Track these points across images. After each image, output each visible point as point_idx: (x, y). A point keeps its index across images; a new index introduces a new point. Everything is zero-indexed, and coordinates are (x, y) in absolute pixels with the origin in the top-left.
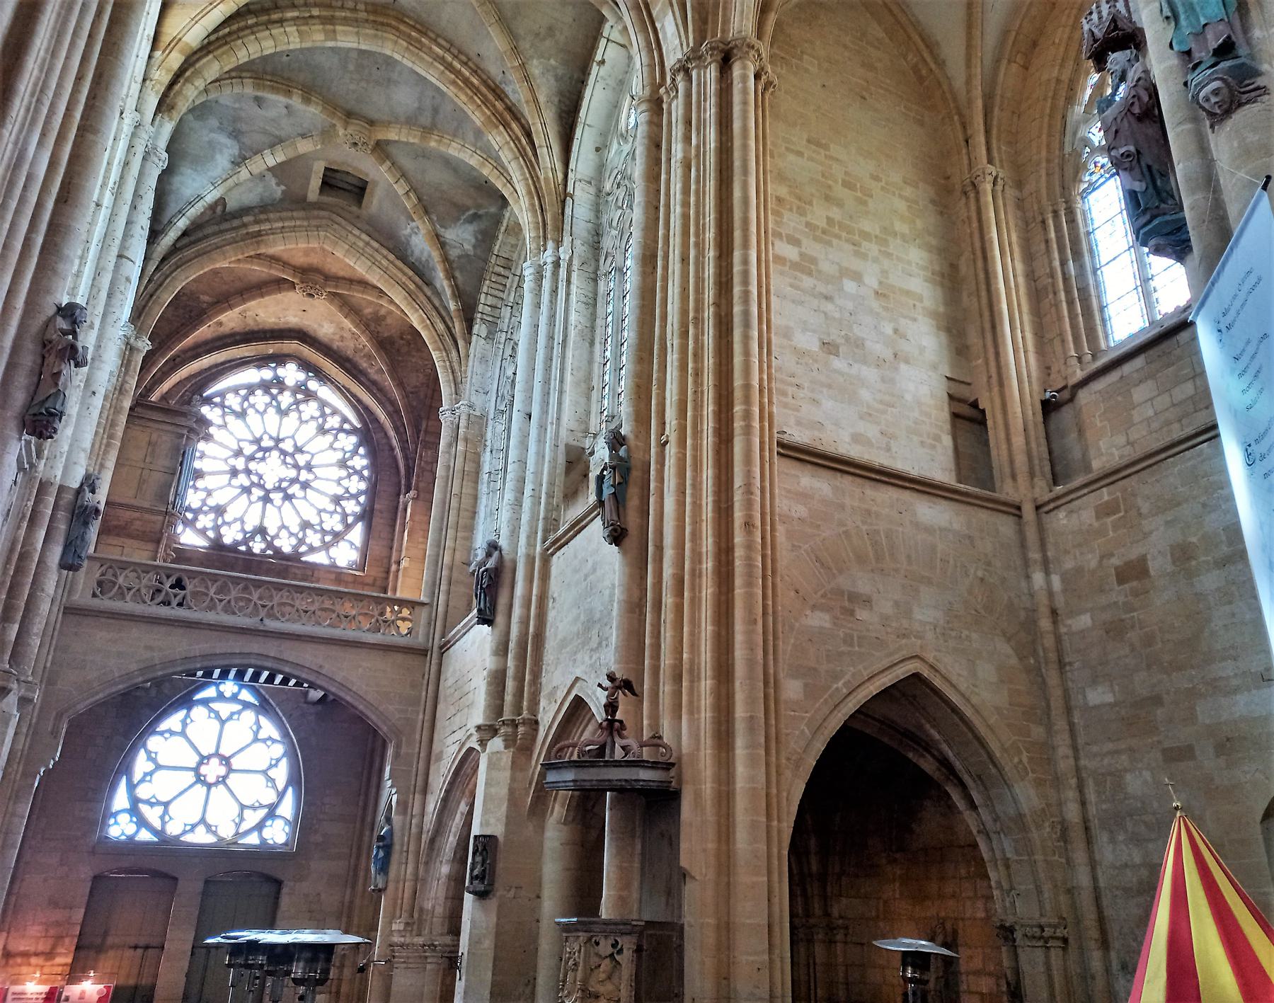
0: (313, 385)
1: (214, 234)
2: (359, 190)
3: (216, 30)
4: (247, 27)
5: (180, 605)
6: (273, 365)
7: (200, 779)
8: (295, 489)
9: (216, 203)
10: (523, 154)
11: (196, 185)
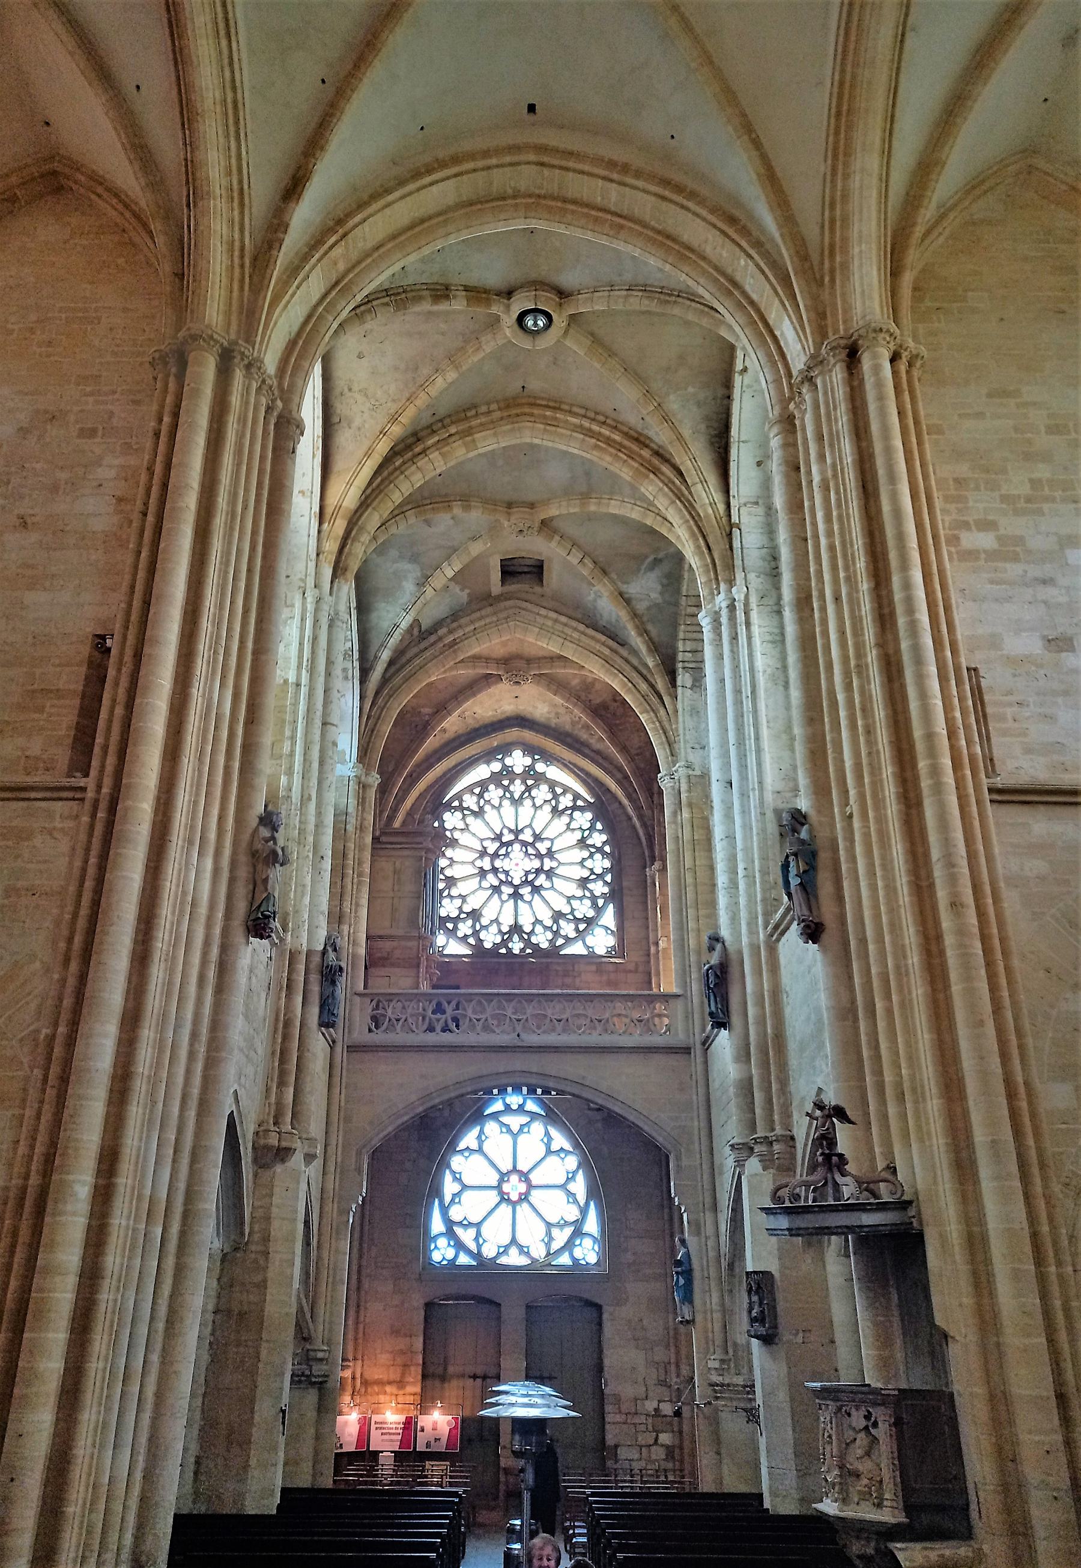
0: (540, 767)
1: (416, 655)
2: (537, 570)
3: (366, 488)
4: (396, 469)
5: (444, 1030)
6: (500, 757)
7: (504, 1198)
8: (541, 880)
9: (411, 627)
10: (679, 496)
11: (390, 615)
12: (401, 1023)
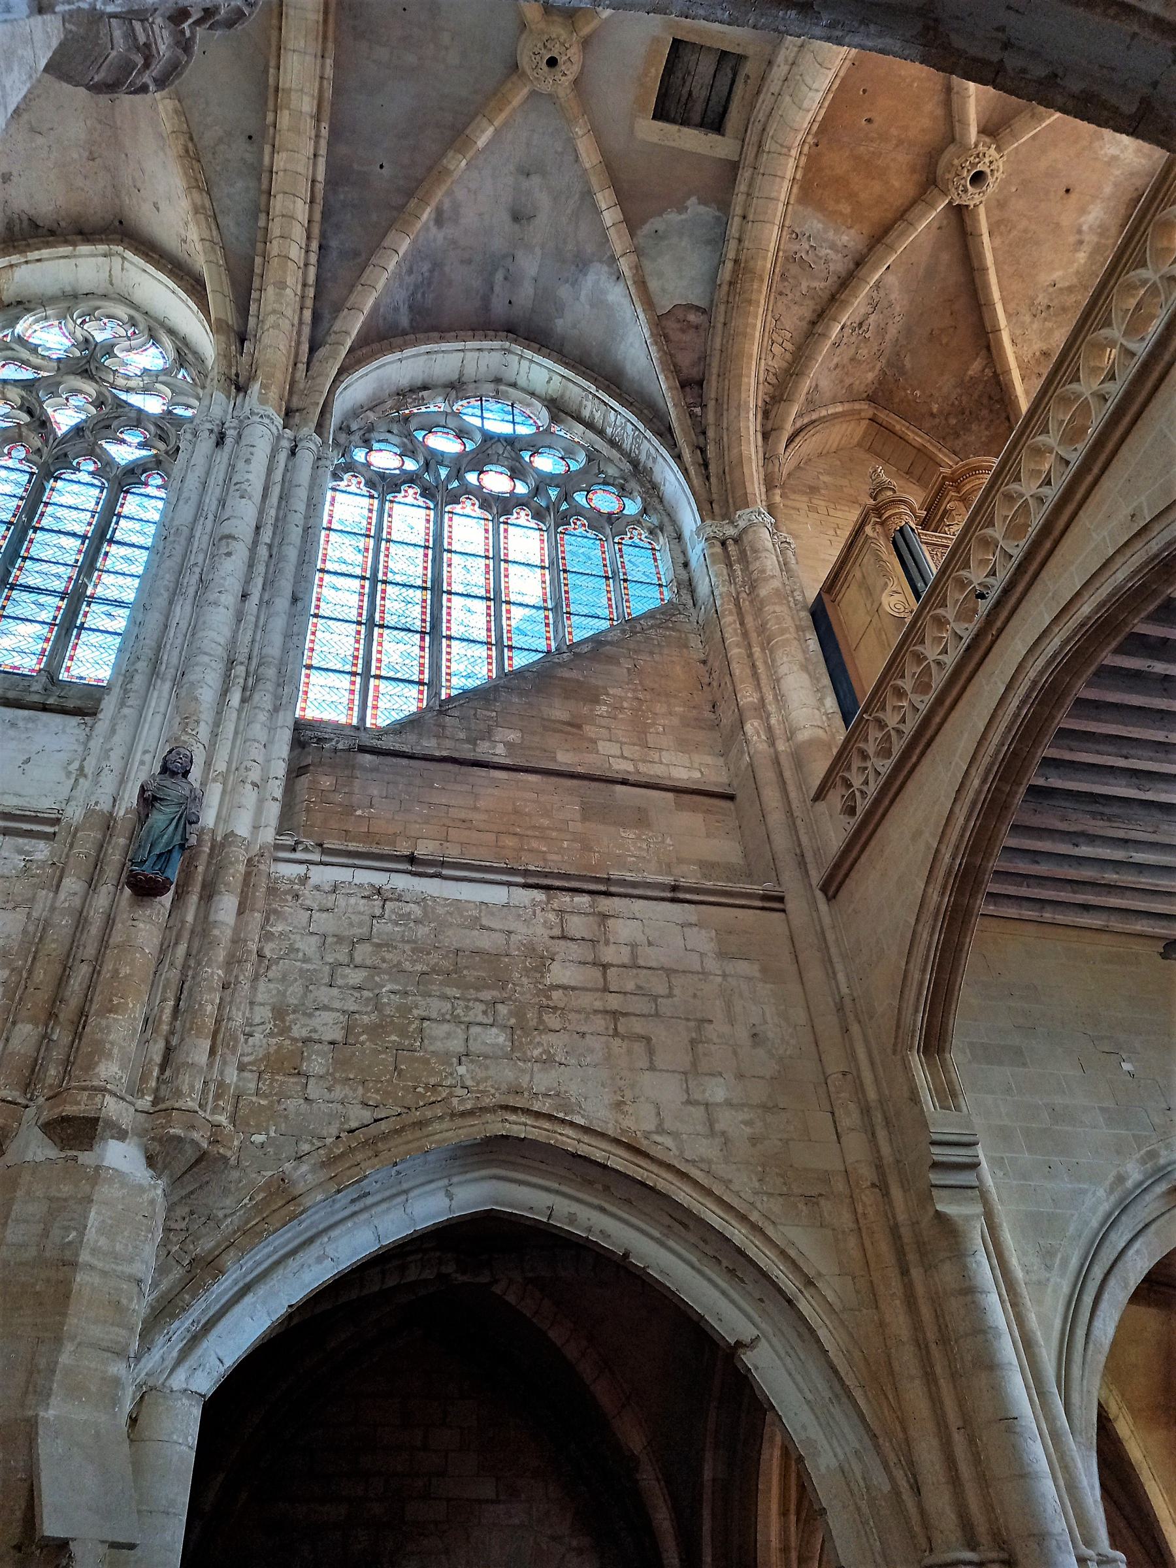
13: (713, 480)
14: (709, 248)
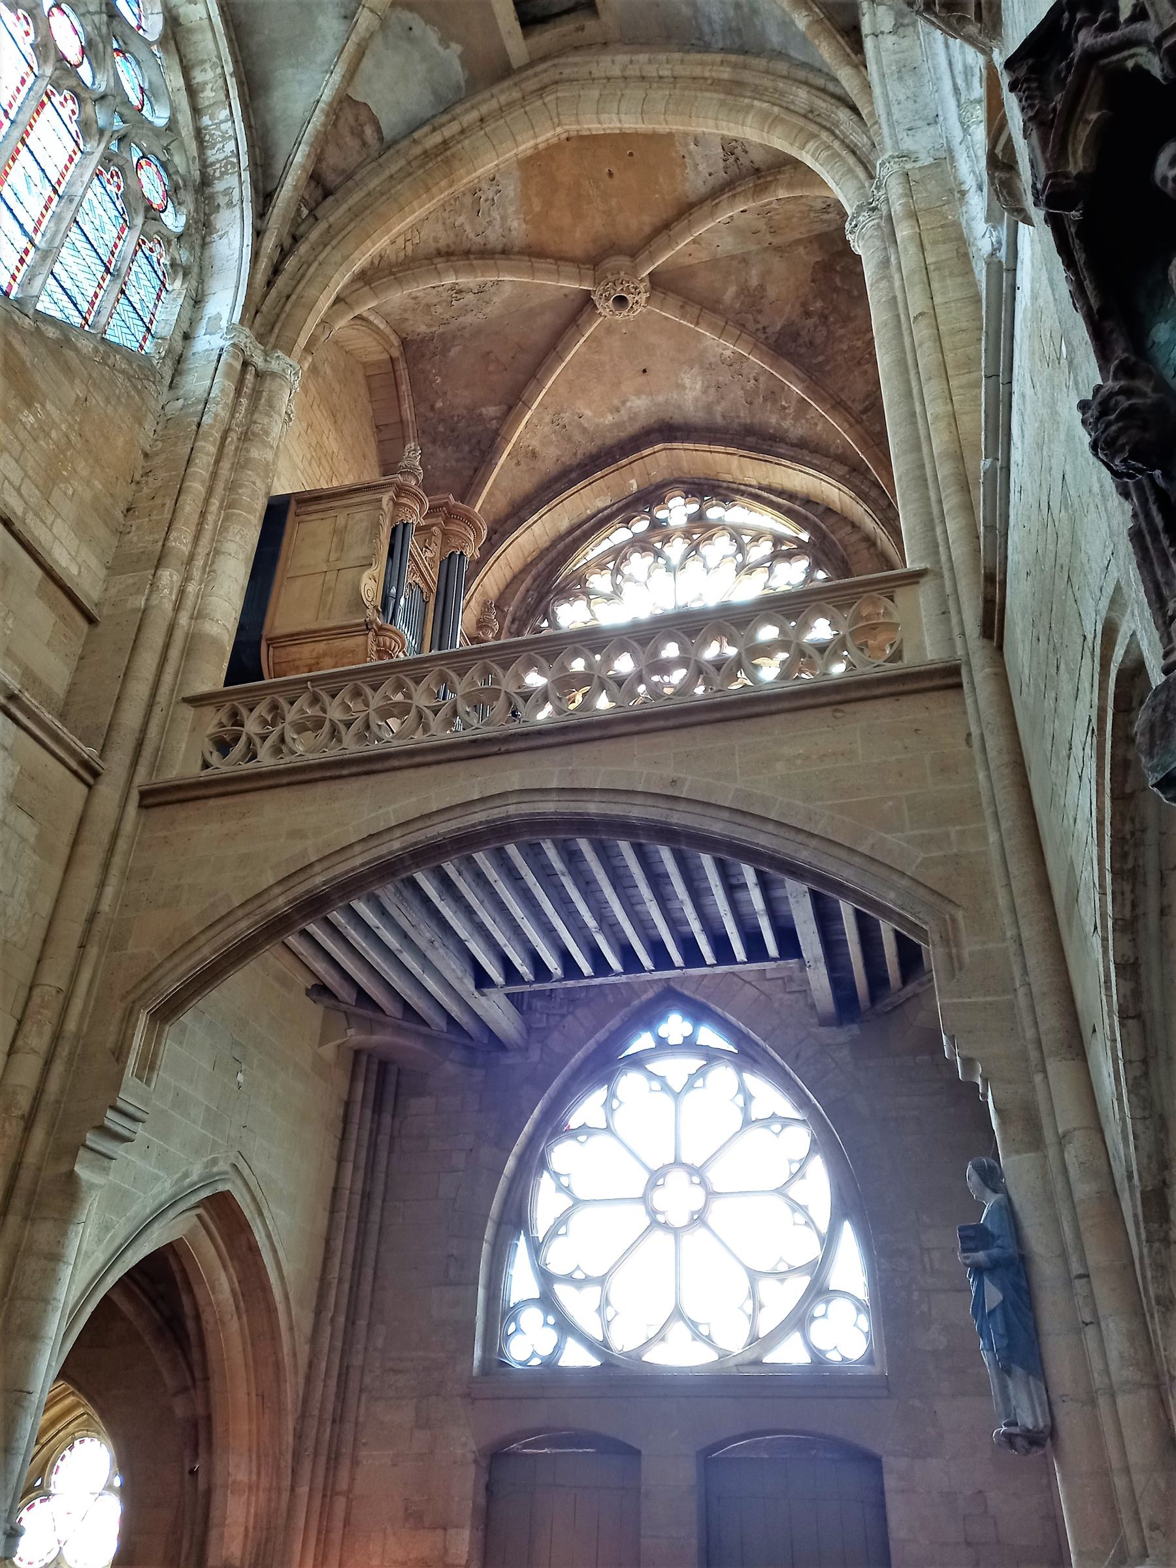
0: (714, 513)
7: (656, 1223)
11: (306, 89)
12: (269, 742)
13: (274, 292)
14: (432, 98)
